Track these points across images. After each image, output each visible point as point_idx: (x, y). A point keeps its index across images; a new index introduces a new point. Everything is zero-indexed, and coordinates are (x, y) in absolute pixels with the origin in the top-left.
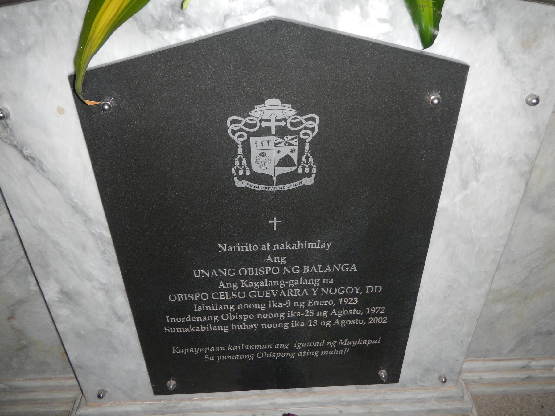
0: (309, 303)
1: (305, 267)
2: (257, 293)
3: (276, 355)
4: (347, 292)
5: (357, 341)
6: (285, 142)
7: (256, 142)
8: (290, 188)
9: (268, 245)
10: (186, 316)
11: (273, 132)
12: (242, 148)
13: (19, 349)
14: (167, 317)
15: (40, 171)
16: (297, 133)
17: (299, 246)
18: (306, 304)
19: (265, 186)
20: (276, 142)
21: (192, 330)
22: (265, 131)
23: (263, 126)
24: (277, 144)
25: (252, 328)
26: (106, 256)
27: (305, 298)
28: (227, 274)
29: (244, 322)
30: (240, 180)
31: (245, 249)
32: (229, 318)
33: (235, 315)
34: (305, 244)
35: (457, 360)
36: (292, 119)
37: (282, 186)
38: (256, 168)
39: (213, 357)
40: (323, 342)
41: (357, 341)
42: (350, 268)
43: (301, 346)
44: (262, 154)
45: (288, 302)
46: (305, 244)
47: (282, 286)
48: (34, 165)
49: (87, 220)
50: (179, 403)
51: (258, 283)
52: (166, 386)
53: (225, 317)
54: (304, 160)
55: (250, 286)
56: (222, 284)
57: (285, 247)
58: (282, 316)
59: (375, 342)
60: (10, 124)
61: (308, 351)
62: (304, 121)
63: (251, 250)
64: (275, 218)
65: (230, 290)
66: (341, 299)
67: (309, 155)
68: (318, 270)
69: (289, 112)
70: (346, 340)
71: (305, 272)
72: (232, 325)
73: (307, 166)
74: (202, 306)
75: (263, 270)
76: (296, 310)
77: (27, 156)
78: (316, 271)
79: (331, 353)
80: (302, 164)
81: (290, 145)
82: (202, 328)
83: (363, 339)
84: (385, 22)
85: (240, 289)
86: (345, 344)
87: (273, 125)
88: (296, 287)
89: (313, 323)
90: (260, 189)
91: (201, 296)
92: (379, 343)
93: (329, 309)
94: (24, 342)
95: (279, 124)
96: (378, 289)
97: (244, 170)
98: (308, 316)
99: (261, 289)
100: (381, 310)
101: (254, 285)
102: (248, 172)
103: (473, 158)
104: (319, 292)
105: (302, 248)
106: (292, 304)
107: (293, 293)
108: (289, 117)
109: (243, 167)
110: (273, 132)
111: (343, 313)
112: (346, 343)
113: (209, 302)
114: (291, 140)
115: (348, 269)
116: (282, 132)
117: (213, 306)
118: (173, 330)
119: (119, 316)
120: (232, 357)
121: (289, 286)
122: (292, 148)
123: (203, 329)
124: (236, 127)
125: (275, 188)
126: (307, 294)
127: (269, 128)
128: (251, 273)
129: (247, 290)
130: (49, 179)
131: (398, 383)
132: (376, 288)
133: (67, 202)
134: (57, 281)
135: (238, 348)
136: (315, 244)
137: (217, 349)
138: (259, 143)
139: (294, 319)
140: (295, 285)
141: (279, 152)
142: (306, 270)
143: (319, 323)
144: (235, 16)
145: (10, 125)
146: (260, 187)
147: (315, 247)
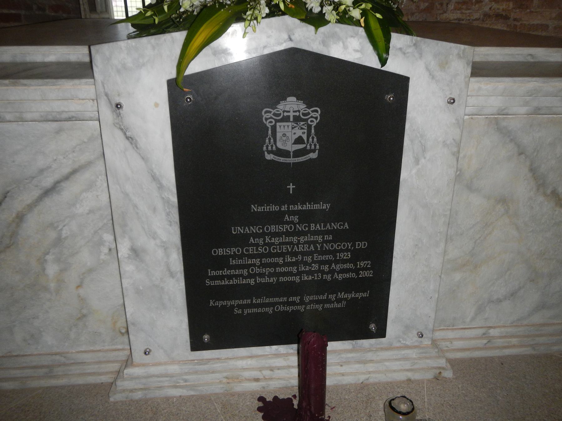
0: (315, 258)
1: (311, 225)
2: (277, 248)
3: (290, 308)
4: (342, 247)
5: (351, 294)
6: (298, 127)
7: (280, 126)
8: (302, 160)
9: (286, 206)
11: (291, 119)
12: (271, 130)
13: (79, 318)
14: (209, 270)
15: (135, 148)
16: (306, 120)
17: (308, 207)
18: (312, 259)
19: (285, 159)
20: (293, 127)
21: (227, 283)
22: (286, 119)
23: (285, 115)
24: (294, 128)
25: (272, 281)
26: (169, 217)
27: (311, 253)
28: (256, 231)
29: (267, 275)
30: (269, 154)
31: (270, 209)
32: (256, 272)
33: (260, 268)
34: (312, 205)
35: (430, 317)
36: (303, 111)
37: (296, 159)
38: (280, 145)
39: (241, 310)
40: (326, 295)
41: (351, 294)
42: (344, 225)
43: (309, 299)
44: (284, 135)
45: (300, 257)
46: (312, 205)
47: (295, 242)
48: (131, 143)
49: (161, 187)
50: (209, 362)
51: (278, 238)
52: (202, 340)
53: (252, 270)
54: (311, 140)
55: (272, 242)
56: (252, 240)
57: (298, 208)
58: (295, 270)
59: (365, 295)
60: (122, 113)
61: (314, 305)
62: (311, 113)
63: (274, 210)
64: (291, 184)
65: (257, 245)
66: (338, 254)
67: (314, 136)
68: (321, 228)
69: (302, 106)
70: (343, 293)
71: (311, 229)
72: (257, 278)
73: (313, 144)
74: (236, 260)
75: (282, 227)
76: (306, 264)
77: (128, 137)
78: (319, 229)
79: (332, 306)
80: (310, 143)
81: (302, 128)
82: (234, 281)
83: (356, 292)
84: (358, 52)
85: (265, 244)
86: (342, 297)
87: (291, 114)
88: (305, 243)
89: (318, 276)
90: (281, 161)
91: (236, 251)
92: (368, 296)
93: (329, 262)
94: (85, 311)
95: (295, 114)
96: (365, 244)
97: (272, 146)
98: (314, 269)
99: (280, 244)
100: (368, 264)
101: (275, 240)
102: (274, 148)
103: (420, 142)
104: (322, 247)
105: (310, 208)
106: (303, 259)
107: (303, 248)
108: (301, 109)
109: (271, 144)
110: (291, 119)
111: (340, 267)
112: (343, 296)
113: (241, 257)
114: (302, 125)
115: (342, 227)
116: (297, 119)
117: (244, 260)
118: (212, 283)
119: (172, 272)
120: (255, 310)
121: (301, 242)
122: (303, 131)
124: (268, 115)
125: (291, 160)
126: (313, 250)
127: (289, 117)
128: (273, 230)
129: (270, 245)
130: (140, 154)
131: (385, 338)
132: (363, 244)
133: (149, 172)
134: (131, 239)
135: (261, 301)
136: (319, 205)
137: (245, 302)
138: (282, 127)
139: (303, 272)
140: (304, 241)
141: (295, 134)
142: (313, 228)
143: (322, 277)
144: (270, 47)
145: (121, 115)
146: (282, 160)
147: (319, 208)
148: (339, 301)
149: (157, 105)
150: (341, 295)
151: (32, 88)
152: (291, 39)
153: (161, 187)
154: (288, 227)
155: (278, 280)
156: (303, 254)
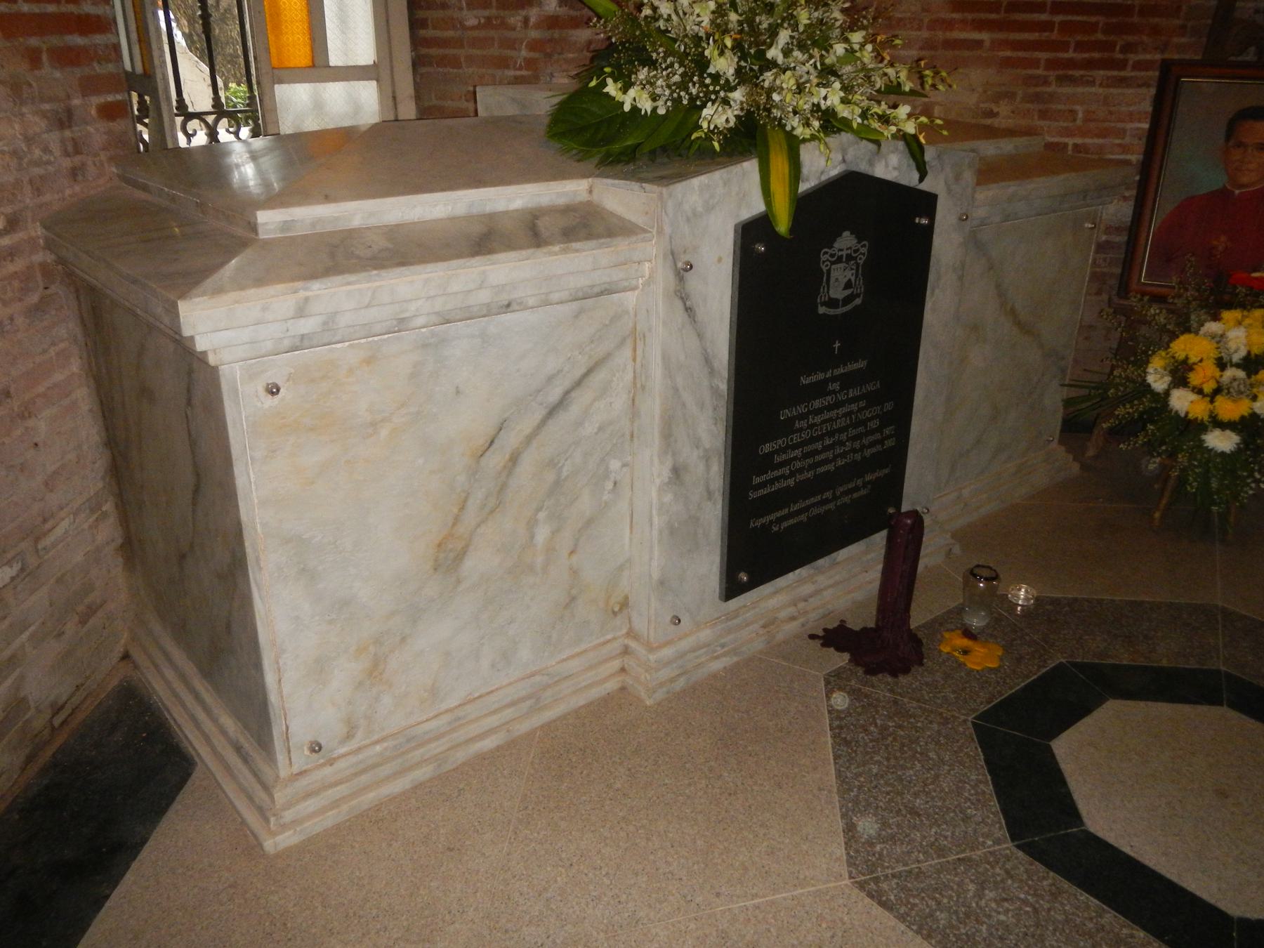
10: (767, 473)
22: (839, 260)
48: (689, 316)
65: (801, 430)
123: (777, 486)
134: (674, 454)
149: (720, 260)
150: (869, 477)
151: (584, 253)
153: (712, 372)
154: (829, 398)
155: (815, 472)
156: (840, 431)
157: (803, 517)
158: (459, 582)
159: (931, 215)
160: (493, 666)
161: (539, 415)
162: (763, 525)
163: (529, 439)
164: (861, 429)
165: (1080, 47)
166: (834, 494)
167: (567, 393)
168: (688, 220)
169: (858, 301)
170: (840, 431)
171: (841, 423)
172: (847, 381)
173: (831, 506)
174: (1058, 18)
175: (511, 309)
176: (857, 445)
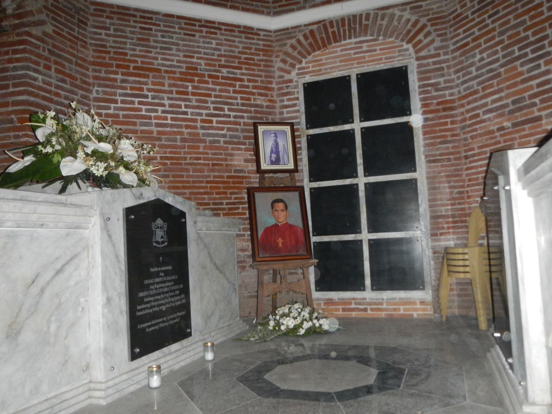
22: (158, 228)
49: (119, 262)
65: (152, 289)
134: (107, 292)
148: (178, 317)
149: (118, 220)
150: (179, 314)
152: (155, 196)
153: (119, 262)
154: (161, 278)
156: (167, 292)
157: (157, 327)
158: (17, 345)
159: (185, 218)
160: (31, 392)
161: (52, 273)
162: (143, 328)
163: (48, 283)
164: (173, 294)
165: (217, 193)
166: (167, 319)
167: (63, 266)
168: (107, 203)
169: (166, 244)
170: (167, 292)
171: (166, 290)
172: (167, 273)
173: (166, 324)
174: (209, 185)
175: (43, 227)
176: (173, 299)
